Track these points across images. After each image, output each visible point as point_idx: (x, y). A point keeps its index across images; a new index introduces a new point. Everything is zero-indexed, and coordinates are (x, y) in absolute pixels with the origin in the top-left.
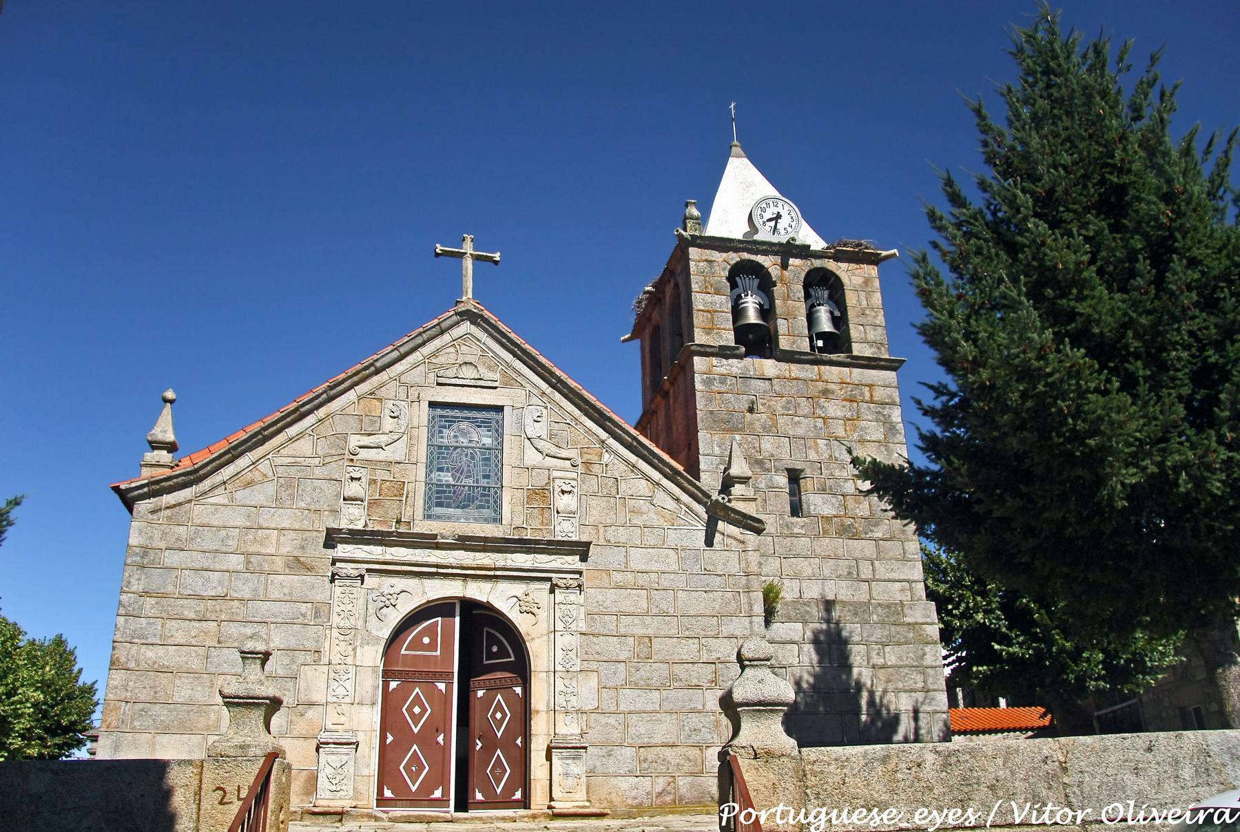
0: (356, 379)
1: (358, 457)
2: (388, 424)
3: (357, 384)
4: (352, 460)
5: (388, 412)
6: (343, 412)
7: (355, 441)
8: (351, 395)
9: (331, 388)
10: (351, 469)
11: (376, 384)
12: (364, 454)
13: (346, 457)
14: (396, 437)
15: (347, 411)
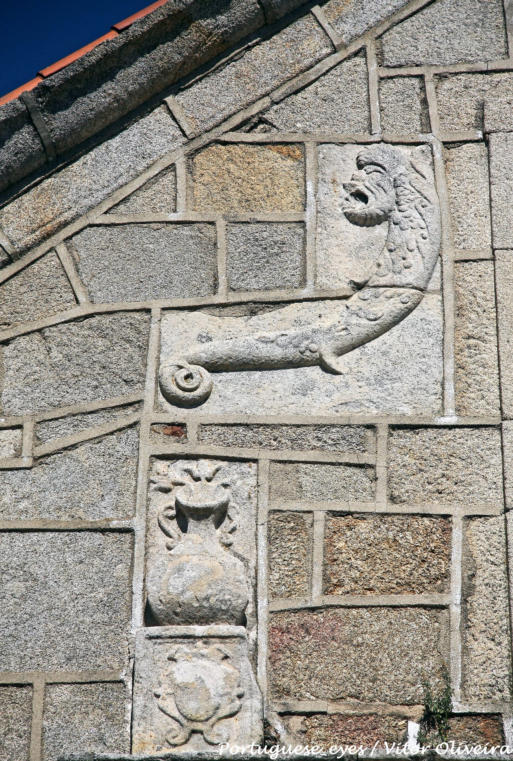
0: (169, 53)
1: (209, 412)
2: (342, 252)
3: (178, 80)
4: (177, 429)
5: (337, 200)
6: (116, 215)
7: (182, 340)
8: (154, 134)
9: (55, 98)
10: (175, 471)
11: (268, 79)
12: (233, 397)
13: (148, 415)
14: (386, 307)
15: (141, 209)
